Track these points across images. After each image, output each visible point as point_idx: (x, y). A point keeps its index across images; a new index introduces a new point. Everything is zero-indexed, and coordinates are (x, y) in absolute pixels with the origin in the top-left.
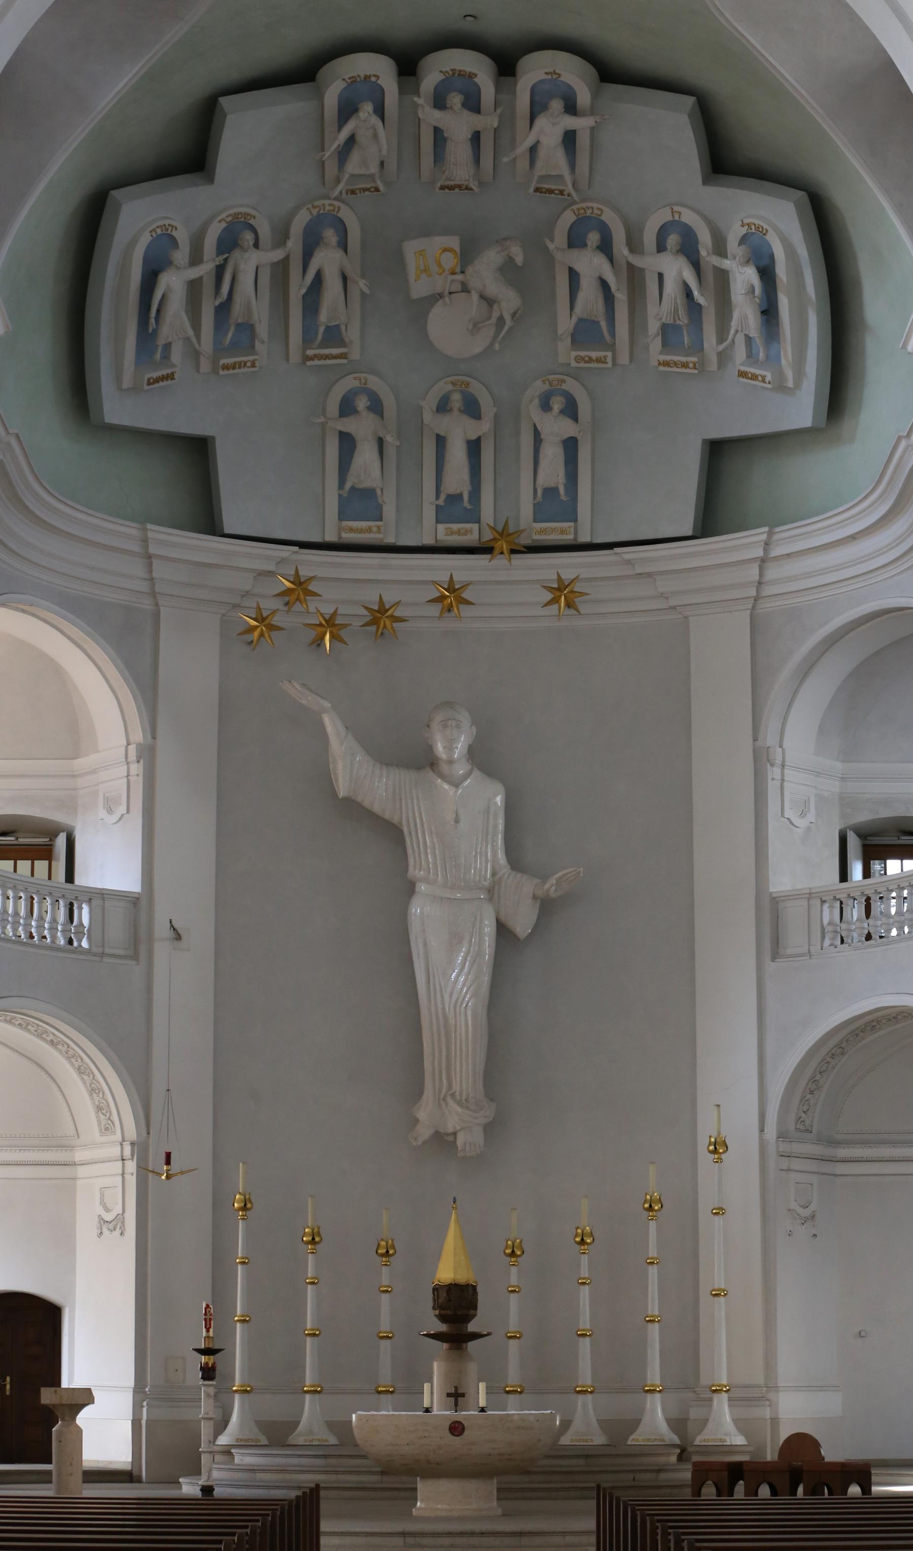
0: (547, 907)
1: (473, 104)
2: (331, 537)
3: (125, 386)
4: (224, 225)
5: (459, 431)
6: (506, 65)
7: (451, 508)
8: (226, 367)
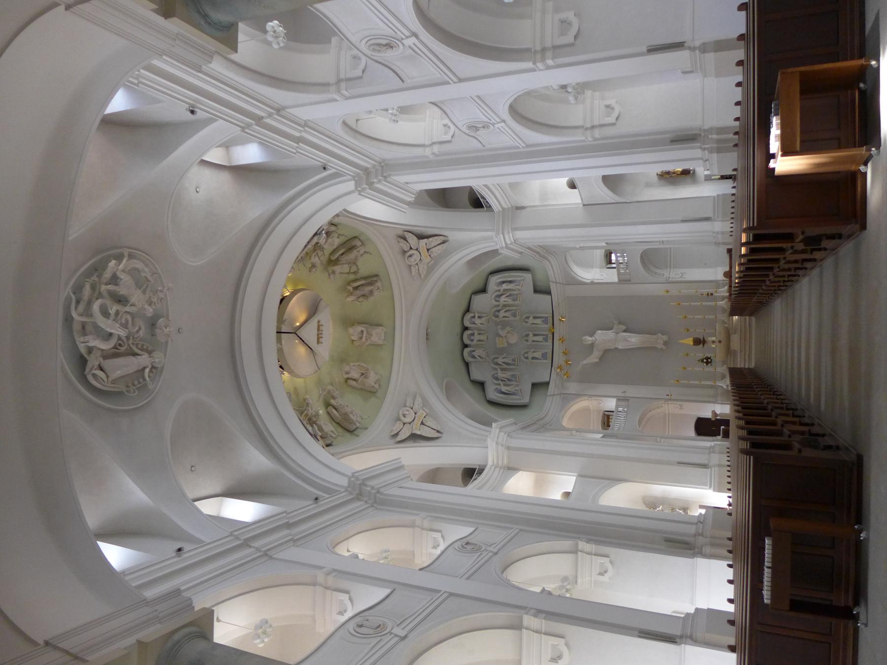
0: (620, 323)
5: (531, 338)
6: (466, 328)
7: (546, 340)
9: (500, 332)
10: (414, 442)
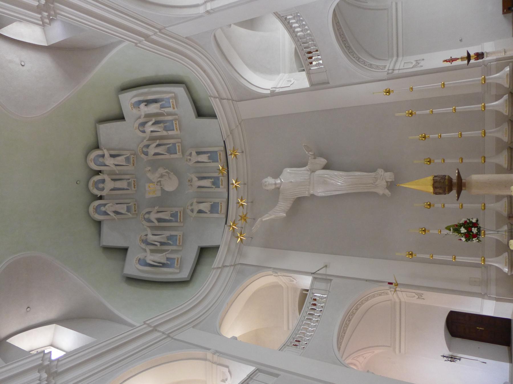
1: (103, 181)
2: (224, 216)
3: (178, 271)
4: (142, 244)
8: (179, 243)
9: (149, 175)
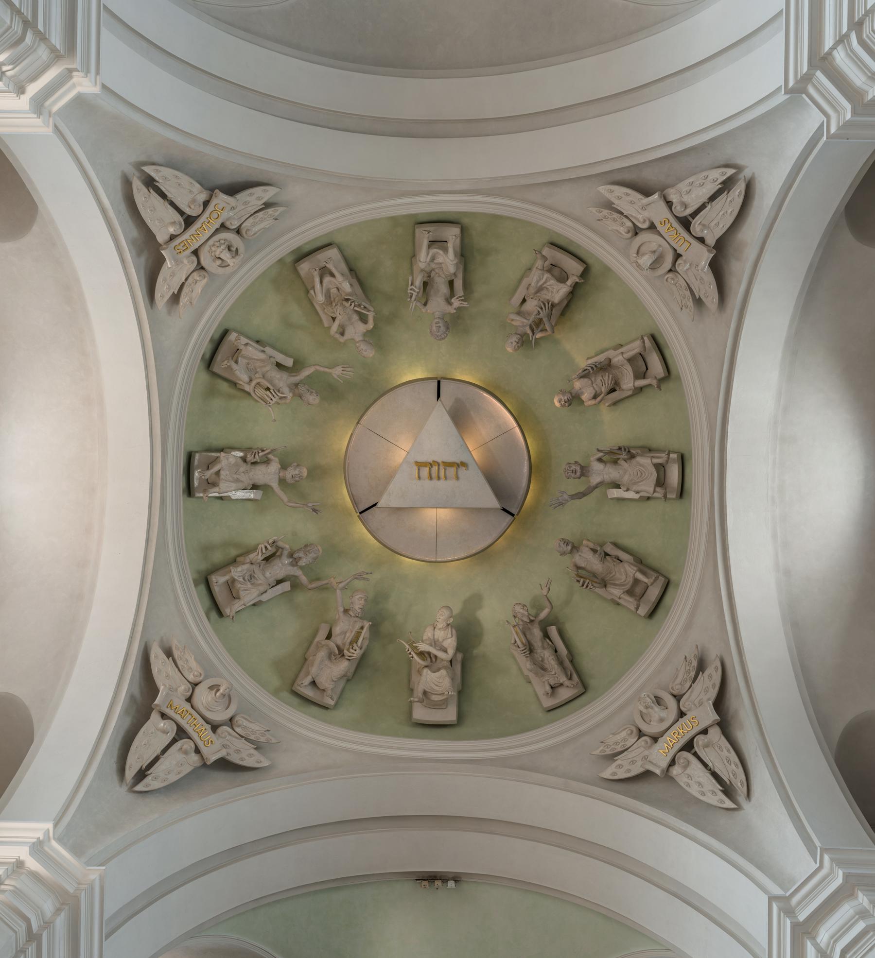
10: (132, 698)
